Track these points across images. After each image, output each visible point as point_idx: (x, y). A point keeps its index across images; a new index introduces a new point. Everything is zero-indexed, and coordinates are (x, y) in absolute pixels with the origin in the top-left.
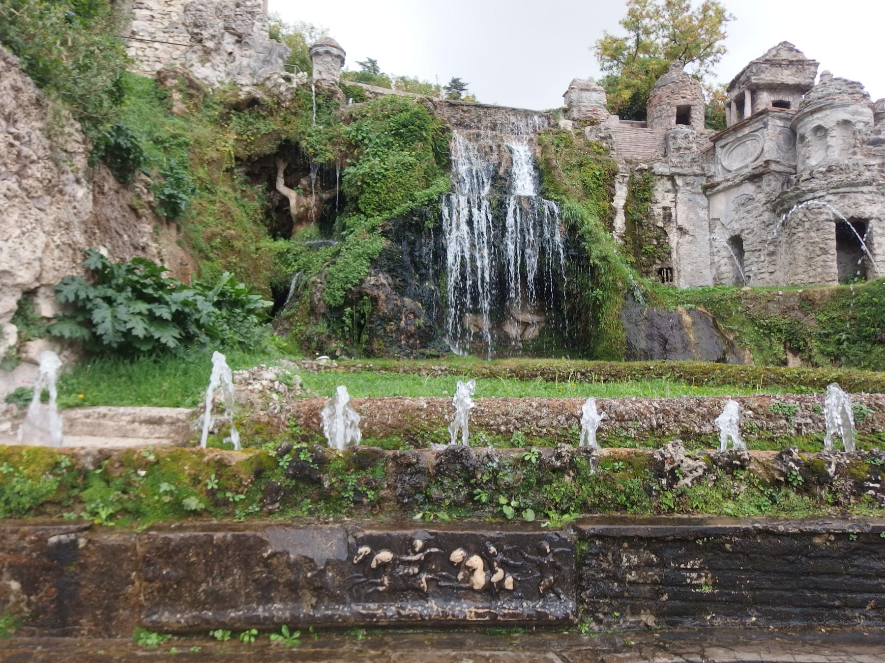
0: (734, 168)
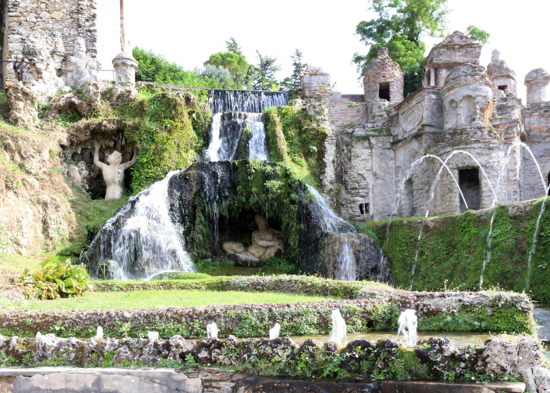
0: (408, 130)
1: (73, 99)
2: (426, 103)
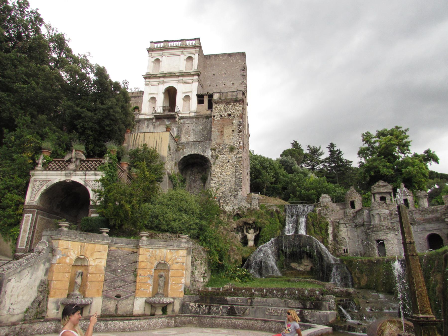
1: (238, 212)
2: (365, 213)
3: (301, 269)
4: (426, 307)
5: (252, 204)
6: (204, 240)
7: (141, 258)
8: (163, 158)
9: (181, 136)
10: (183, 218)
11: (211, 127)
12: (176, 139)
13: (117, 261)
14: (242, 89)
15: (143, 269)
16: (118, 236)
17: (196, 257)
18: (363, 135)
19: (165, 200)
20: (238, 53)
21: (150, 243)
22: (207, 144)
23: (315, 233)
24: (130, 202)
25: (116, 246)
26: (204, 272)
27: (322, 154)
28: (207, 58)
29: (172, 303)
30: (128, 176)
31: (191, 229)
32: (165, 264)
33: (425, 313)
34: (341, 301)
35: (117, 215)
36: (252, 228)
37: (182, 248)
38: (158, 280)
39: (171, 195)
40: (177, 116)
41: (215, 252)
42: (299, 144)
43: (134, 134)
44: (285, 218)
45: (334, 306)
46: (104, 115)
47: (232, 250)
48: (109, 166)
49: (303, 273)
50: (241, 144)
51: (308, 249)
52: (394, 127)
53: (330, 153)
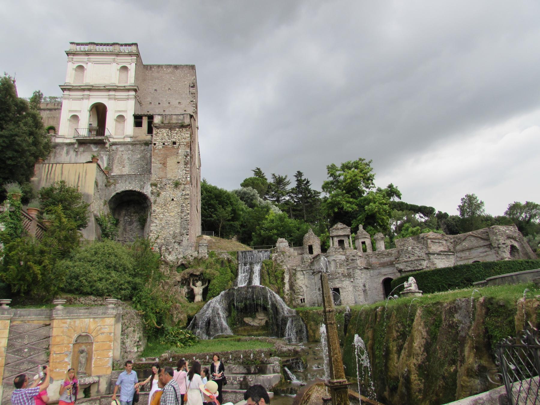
1: (183, 262)
3: (255, 324)
4: (340, 372)
5: (200, 252)
6: (138, 302)
7: (55, 332)
8: (88, 196)
9: (112, 166)
10: (112, 277)
11: (151, 156)
12: (106, 172)
13: (22, 338)
14: (190, 111)
15: (58, 344)
16: (23, 305)
17: (127, 324)
18: (328, 168)
19: (88, 255)
20: (187, 65)
21: (68, 312)
22: (146, 178)
23: (270, 282)
24: (40, 263)
25: (21, 319)
26: (138, 340)
27: (288, 183)
28: (147, 69)
29: (97, 383)
30: (38, 225)
31: (121, 289)
32: (87, 336)
33: (339, 378)
34: (288, 361)
35: (23, 279)
36: (199, 280)
37: (109, 316)
38: (78, 356)
39: (96, 248)
40: (107, 141)
41: (151, 315)
42: (263, 172)
43: (47, 165)
44: (238, 266)
45: (278, 369)
46: (4, 144)
47: (175, 308)
48: (10, 215)
49: (257, 328)
50: (189, 179)
51: (261, 302)
52: (358, 160)
53: (297, 183)
